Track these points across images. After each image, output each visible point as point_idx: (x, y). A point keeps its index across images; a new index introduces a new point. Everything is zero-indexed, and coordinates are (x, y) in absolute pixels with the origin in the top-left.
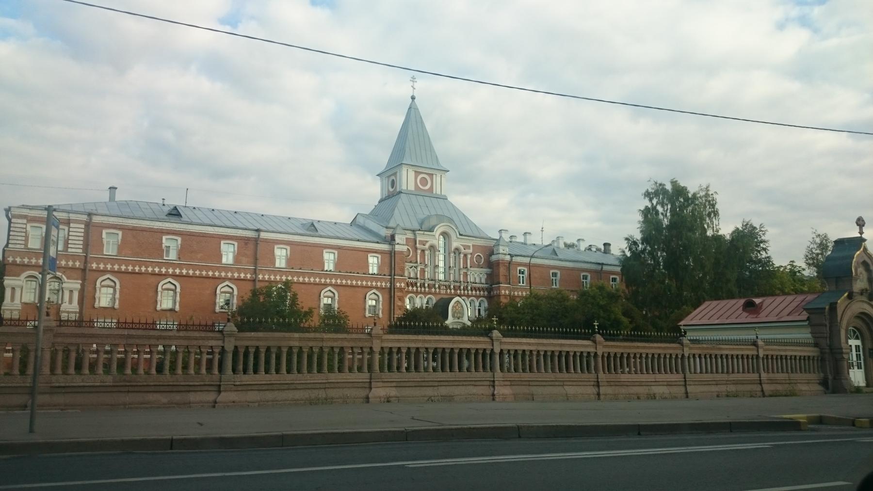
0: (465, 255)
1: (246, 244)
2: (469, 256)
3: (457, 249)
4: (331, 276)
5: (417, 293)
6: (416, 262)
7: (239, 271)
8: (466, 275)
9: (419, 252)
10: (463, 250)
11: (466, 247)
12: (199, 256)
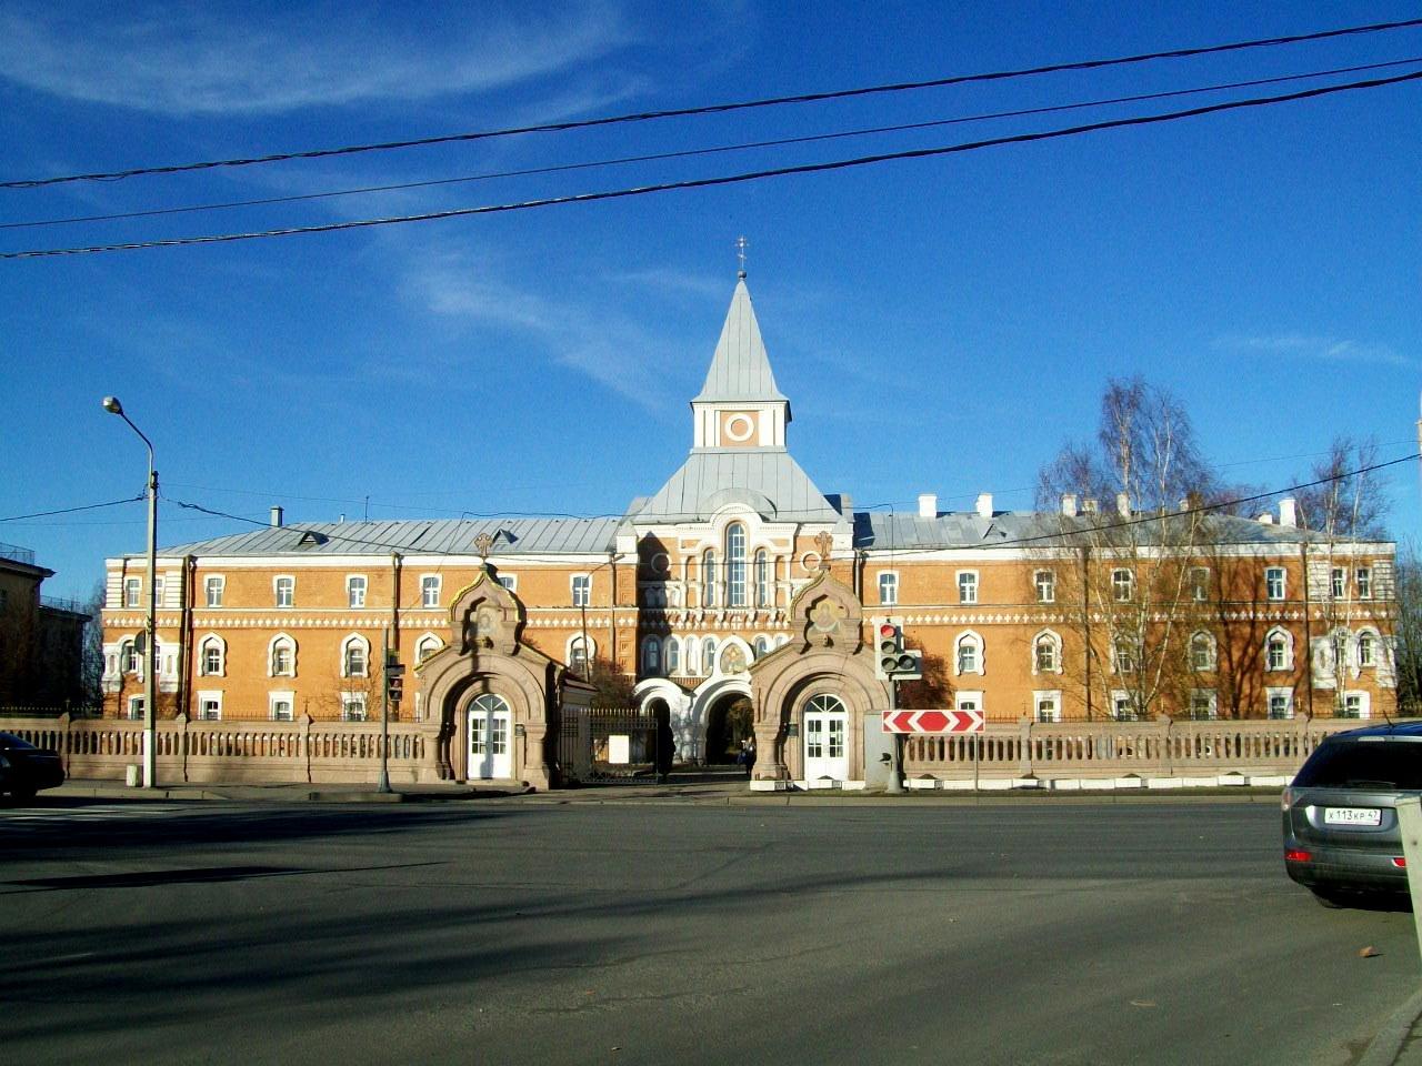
1: (380, 576)
3: (760, 551)
7: (373, 616)
11: (777, 542)
12: (319, 599)
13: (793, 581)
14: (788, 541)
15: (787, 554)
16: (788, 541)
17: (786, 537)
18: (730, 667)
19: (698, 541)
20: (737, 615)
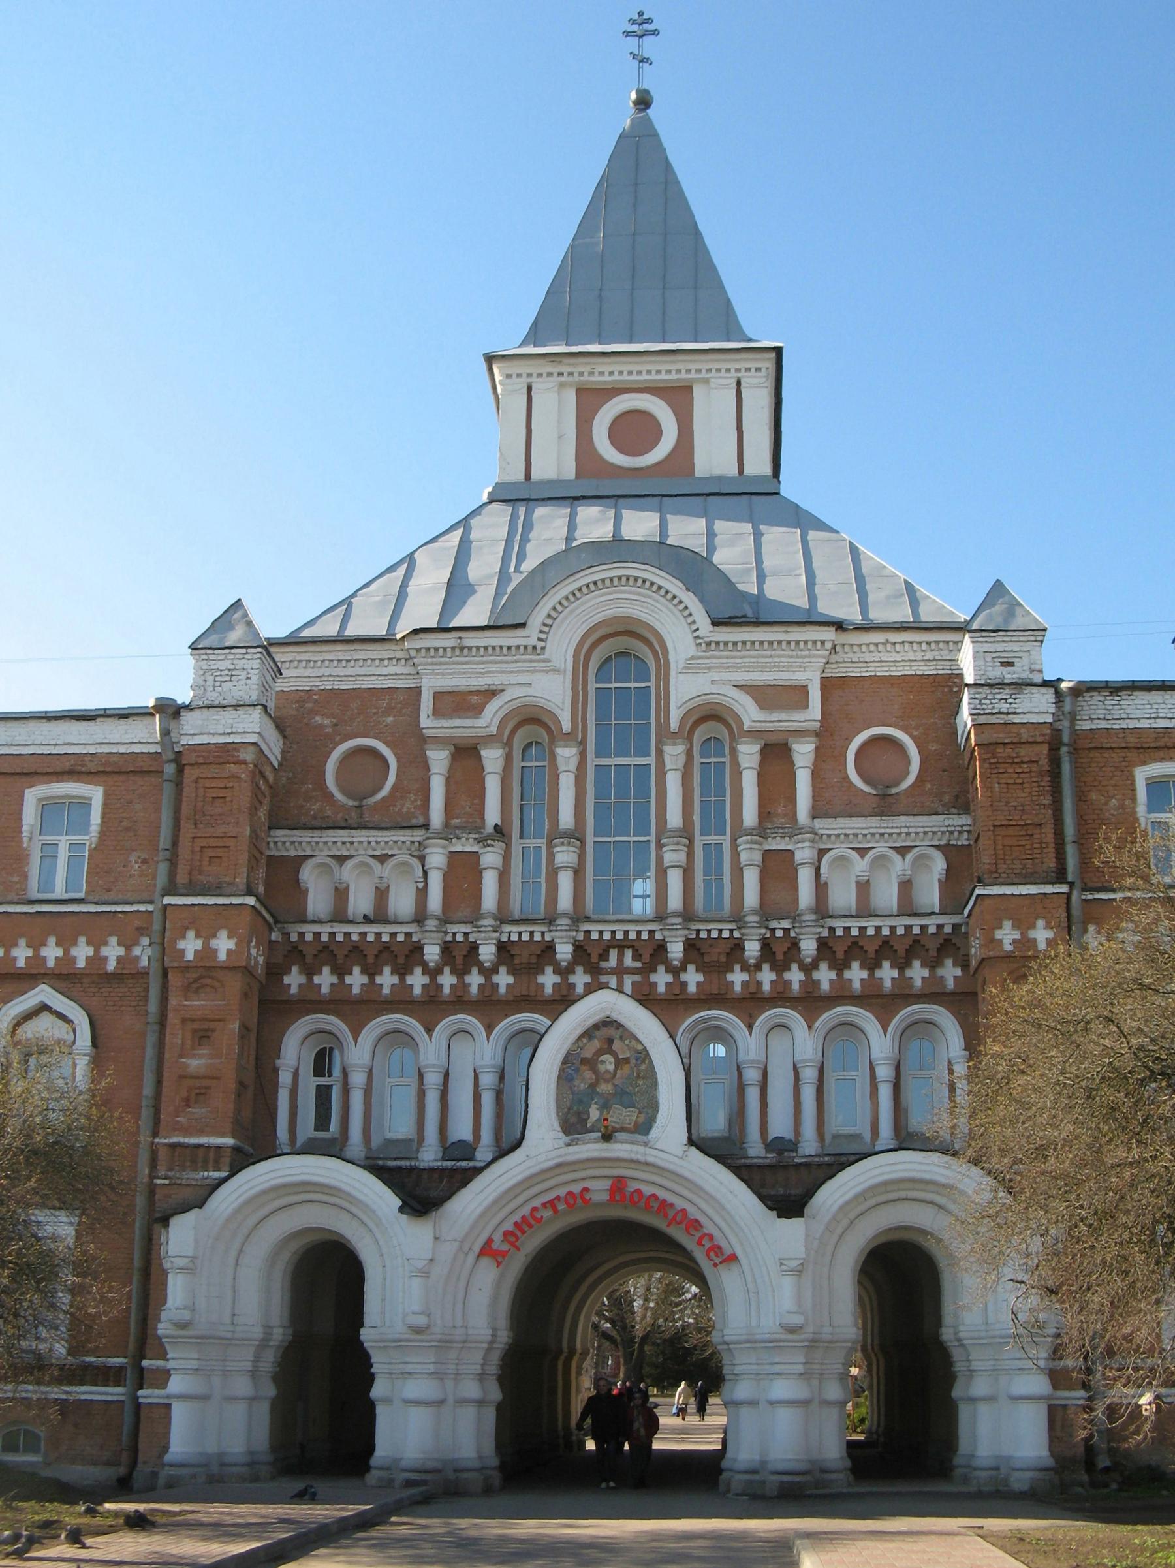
0: (776, 753)
2: (803, 752)
3: (710, 715)
5: (431, 1008)
6: (426, 826)
8: (777, 869)
9: (439, 759)
10: (750, 713)
14: (803, 690)
16: (803, 690)
17: (799, 677)
18: (594, 1114)
19: (491, 693)
20: (621, 946)
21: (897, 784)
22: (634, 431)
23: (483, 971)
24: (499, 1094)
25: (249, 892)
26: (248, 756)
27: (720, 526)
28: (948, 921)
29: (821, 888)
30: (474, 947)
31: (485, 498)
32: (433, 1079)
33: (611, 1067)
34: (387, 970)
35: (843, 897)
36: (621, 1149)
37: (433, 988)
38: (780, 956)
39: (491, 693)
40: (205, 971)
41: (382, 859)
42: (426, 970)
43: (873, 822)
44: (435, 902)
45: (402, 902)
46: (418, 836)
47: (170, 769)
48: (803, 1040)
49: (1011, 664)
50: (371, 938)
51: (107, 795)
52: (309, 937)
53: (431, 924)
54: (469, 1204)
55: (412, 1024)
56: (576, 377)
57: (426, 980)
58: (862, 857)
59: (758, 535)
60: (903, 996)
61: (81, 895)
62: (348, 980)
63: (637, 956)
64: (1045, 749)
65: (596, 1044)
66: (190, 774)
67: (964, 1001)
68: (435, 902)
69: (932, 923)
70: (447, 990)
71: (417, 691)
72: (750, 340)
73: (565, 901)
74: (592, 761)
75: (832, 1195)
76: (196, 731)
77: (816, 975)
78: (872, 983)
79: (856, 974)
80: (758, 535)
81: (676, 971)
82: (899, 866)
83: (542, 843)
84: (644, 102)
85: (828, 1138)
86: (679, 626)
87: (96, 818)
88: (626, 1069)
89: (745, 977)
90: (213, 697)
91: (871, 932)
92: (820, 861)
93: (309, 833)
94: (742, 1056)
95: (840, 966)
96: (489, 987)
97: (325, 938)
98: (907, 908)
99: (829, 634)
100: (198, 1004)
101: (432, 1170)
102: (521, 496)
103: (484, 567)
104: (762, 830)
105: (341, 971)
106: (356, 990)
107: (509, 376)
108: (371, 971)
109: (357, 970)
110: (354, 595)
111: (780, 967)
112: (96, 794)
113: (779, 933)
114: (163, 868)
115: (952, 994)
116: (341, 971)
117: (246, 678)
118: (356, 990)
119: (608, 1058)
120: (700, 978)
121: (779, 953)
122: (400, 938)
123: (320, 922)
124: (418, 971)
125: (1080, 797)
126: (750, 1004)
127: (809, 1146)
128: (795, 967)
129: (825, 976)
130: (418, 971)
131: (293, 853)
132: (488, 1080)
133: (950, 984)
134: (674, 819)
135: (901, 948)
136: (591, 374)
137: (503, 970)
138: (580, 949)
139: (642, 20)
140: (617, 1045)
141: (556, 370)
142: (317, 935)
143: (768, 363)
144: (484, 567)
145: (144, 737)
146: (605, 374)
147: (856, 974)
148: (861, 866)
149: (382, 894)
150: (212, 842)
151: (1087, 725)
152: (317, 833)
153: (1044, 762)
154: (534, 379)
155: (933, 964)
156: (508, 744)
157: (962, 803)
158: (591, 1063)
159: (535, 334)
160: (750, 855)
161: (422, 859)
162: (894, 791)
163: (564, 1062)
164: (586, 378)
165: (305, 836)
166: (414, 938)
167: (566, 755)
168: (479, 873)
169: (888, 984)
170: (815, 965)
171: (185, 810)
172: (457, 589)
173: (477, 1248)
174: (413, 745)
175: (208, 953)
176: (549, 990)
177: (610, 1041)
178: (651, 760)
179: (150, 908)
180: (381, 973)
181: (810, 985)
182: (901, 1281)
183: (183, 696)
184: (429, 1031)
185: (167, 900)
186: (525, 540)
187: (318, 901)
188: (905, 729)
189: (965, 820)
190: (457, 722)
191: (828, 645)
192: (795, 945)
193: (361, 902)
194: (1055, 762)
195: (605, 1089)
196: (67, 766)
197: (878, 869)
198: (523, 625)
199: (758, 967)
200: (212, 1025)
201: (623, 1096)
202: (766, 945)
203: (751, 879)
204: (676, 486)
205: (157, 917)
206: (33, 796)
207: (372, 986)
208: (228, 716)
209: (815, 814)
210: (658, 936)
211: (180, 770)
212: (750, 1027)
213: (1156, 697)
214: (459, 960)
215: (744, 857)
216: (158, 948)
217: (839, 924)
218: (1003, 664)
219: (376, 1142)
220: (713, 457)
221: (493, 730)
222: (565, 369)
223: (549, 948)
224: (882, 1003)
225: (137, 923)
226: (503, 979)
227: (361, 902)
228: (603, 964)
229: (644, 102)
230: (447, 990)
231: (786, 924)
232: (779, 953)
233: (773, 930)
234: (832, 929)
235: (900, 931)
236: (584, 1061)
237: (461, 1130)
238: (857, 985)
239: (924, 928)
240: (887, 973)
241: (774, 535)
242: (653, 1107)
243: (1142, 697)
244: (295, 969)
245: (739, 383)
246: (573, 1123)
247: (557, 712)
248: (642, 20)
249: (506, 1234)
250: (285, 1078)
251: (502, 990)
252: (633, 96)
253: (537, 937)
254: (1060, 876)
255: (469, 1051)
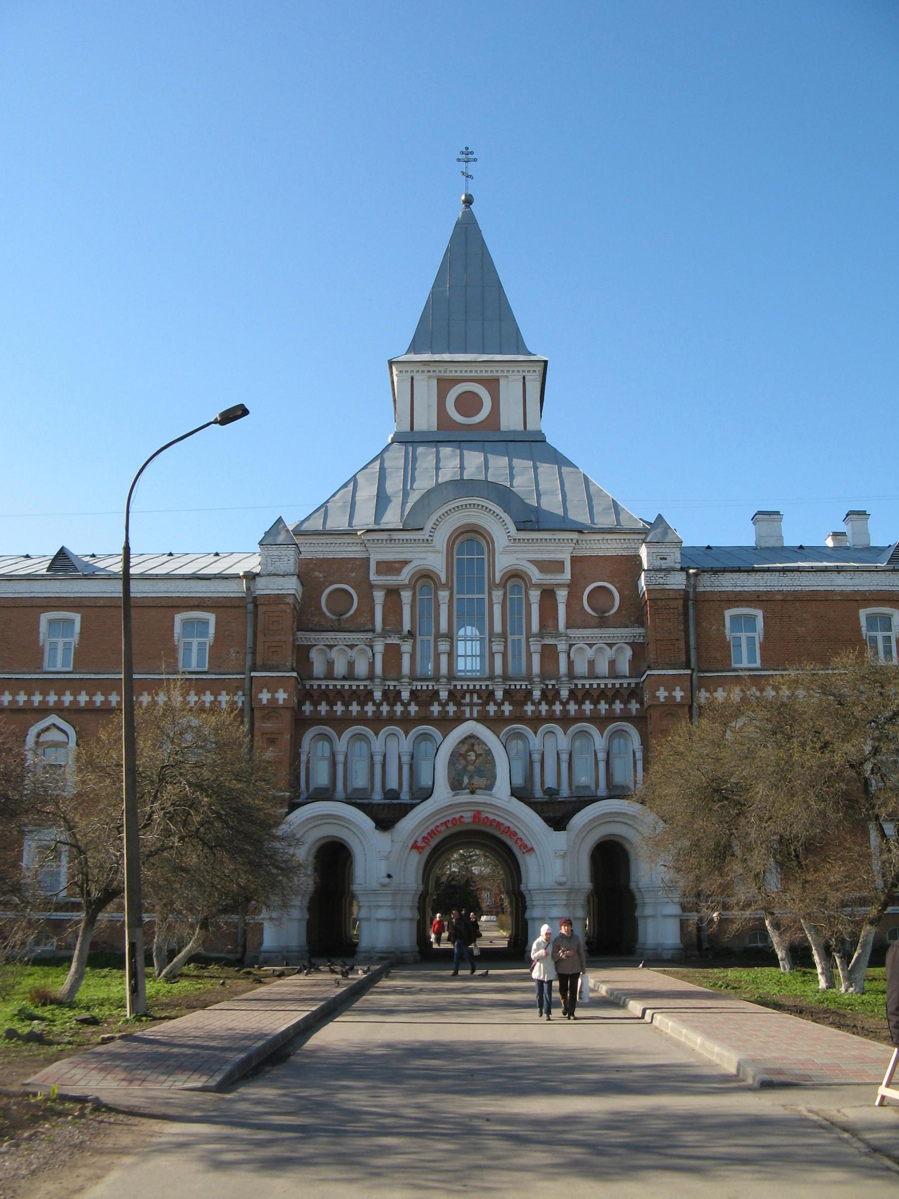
0: (548, 594)
2: (562, 595)
3: (515, 576)
4: (61, 685)
5: (377, 723)
6: (373, 631)
8: (549, 654)
9: (379, 596)
10: (536, 575)
11: (545, 566)
13: (572, 632)
14: (562, 563)
15: (560, 585)
18: (466, 780)
19: (405, 563)
20: (472, 692)
21: (609, 611)
22: (469, 403)
23: (403, 704)
24: (411, 766)
25: (293, 670)
26: (290, 600)
27: (516, 462)
28: (633, 681)
29: (570, 664)
30: (399, 692)
31: (390, 441)
32: (378, 759)
33: (474, 758)
34: (355, 703)
35: (581, 668)
36: (478, 798)
37: (377, 713)
38: (550, 698)
39: (405, 563)
40: (272, 709)
41: (352, 647)
42: (374, 704)
43: (596, 631)
44: (379, 669)
45: (361, 669)
46: (370, 635)
47: (250, 607)
48: (561, 739)
49: (665, 559)
50: (347, 687)
51: (217, 618)
52: (315, 687)
53: (377, 681)
54: (408, 824)
55: (368, 731)
56: (437, 374)
57: (374, 708)
58: (591, 648)
59: (536, 468)
60: (611, 718)
61: (206, 669)
62: (335, 708)
63: (479, 697)
64: (681, 602)
65: (466, 747)
66: (261, 609)
67: (640, 721)
68: (379, 669)
69: (625, 682)
70: (385, 714)
71: (368, 559)
72: (530, 354)
73: (444, 670)
74: (456, 596)
75: (580, 819)
76: (263, 587)
77: (568, 707)
78: (595, 711)
79: (588, 707)
80: (536, 468)
81: (499, 705)
82: (609, 653)
83: (432, 638)
84: (469, 201)
85: (574, 787)
86: (500, 528)
87: (212, 630)
88: (481, 759)
89: (533, 708)
90: (271, 569)
91: (595, 686)
92: (570, 650)
93: (314, 633)
94: (531, 748)
95: (580, 703)
96: (406, 712)
97: (323, 687)
98: (613, 674)
99: (575, 536)
100: (269, 725)
101: (379, 805)
102: (408, 439)
103: (394, 485)
104: (541, 635)
105: (331, 704)
106: (339, 713)
107: (401, 372)
108: (347, 704)
109: (339, 703)
110: (327, 502)
111: (551, 703)
112: (211, 618)
113: (550, 687)
114: (249, 657)
115: (635, 717)
116: (331, 704)
117: (287, 561)
118: (339, 713)
119: (472, 753)
120: (511, 708)
121: (550, 696)
122: (362, 688)
123: (320, 679)
124: (370, 704)
125: (698, 625)
126: (536, 722)
127: (565, 792)
128: (557, 703)
129: (572, 707)
130: (370, 704)
131: (305, 643)
132: (406, 759)
133: (634, 712)
134: (498, 628)
135: (610, 694)
136: (445, 371)
137: (413, 703)
138: (452, 694)
139: (467, 152)
140: (476, 747)
141: (426, 369)
142: (320, 686)
143: (539, 368)
144: (394, 485)
145: (238, 589)
146: (452, 372)
147: (588, 707)
148: (590, 653)
149: (351, 665)
150: (274, 644)
151: (701, 589)
152: (318, 633)
153: (681, 609)
154: (414, 374)
155: (626, 702)
156: (414, 589)
157: (640, 621)
158: (464, 756)
159: (414, 347)
160: (535, 647)
161: (371, 647)
162: (606, 615)
163: (451, 756)
164: (442, 374)
165: (312, 635)
166: (369, 688)
167: (444, 595)
168: (400, 655)
169: (603, 712)
170: (567, 703)
171: (260, 628)
172: (382, 501)
173: (410, 846)
174: (366, 591)
175: (273, 700)
176: (436, 714)
177: (473, 745)
178: (486, 596)
179: (243, 676)
180: (351, 705)
181: (565, 712)
182: (610, 861)
183: (257, 570)
184: (377, 734)
185: (253, 674)
186: (414, 469)
187: (319, 668)
188: (612, 583)
189: (641, 631)
190: (389, 578)
191: (575, 541)
192: (558, 692)
193: (340, 668)
194: (686, 607)
195: (470, 768)
196: (196, 603)
197: (598, 654)
198: (422, 529)
199: (540, 703)
200: (276, 736)
201: (480, 772)
202: (544, 693)
203: (536, 659)
204: (491, 437)
205: (247, 682)
206: (179, 618)
207: (347, 712)
208: (280, 581)
209: (568, 626)
210: (490, 688)
211: (256, 606)
212: (536, 733)
213: (735, 575)
214: (391, 699)
215: (532, 648)
216: (248, 697)
217: (580, 683)
218: (661, 559)
219: (349, 790)
220: (510, 420)
221: (407, 582)
222: (431, 369)
223: (436, 693)
224: (601, 721)
225: (236, 684)
226: (413, 708)
227: (340, 668)
228: (463, 701)
229: (469, 201)
230: (385, 714)
231: (553, 682)
232: (550, 696)
233: (547, 685)
234: (576, 685)
235: (610, 686)
236: (461, 755)
237: (393, 784)
238: (588, 712)
239: (621, 684)
240: (603, 706)
241: (544, 468)
242: (494, 777)
243: (729, 575)
244: (308, 703)
245: (524, 378)
246: (456, 785)
247: (439, 573)
248: (467, 152)
249: (424, 838)
250: (303, 758)
251: (413, 714)
252: (463, 197)
253: (430, 688)
254: (687, 666)
255: (395, 744)
